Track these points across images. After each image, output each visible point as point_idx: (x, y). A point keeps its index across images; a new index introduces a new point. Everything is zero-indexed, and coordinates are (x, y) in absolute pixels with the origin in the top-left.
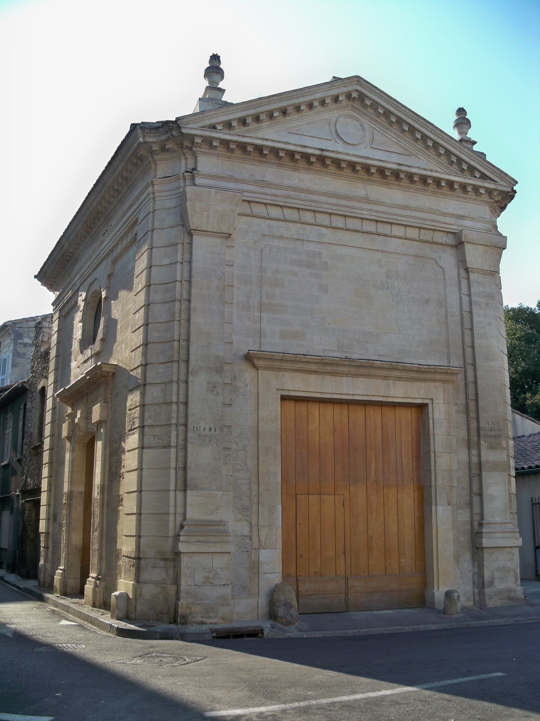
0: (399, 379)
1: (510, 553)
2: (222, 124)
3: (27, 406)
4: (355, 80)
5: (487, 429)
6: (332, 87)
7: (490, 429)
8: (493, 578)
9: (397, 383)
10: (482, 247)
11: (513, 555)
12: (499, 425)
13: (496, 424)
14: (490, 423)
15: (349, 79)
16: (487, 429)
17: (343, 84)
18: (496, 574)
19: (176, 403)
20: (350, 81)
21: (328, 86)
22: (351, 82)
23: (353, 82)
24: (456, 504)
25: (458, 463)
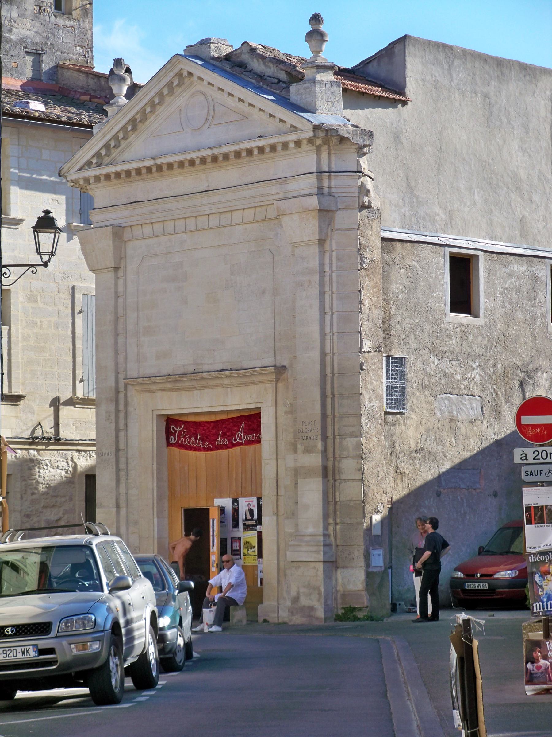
0: (233, 385)
1: (315, 568)
2: (95, 158)
3: (390, 416)
4: (175, 60)
5: (304, 431)
6: (160, 79)
7: (306, 430)
8: (298, 593)
9: (234, 389)
10: (297, 215)
11: (318, 570)
12: (315, 424)
13: (313, 423)
14: (307, 423)
15: (170, 63)
16: (304, 431)
17: (167, 70)
18: (302, 590)
19: (48, 429)
20: (171, 64)
21: (155, 80)
22: (174, 64)
23: (175, 63)
24: (284, 514)
25: (286, 470)
